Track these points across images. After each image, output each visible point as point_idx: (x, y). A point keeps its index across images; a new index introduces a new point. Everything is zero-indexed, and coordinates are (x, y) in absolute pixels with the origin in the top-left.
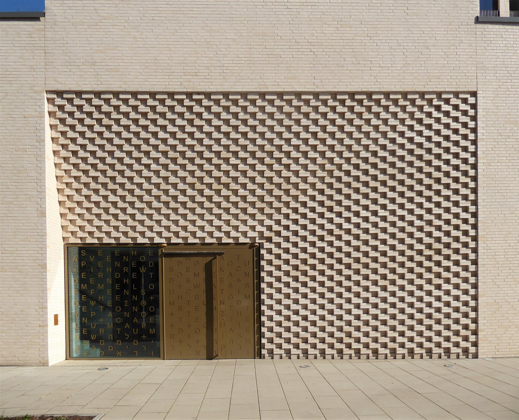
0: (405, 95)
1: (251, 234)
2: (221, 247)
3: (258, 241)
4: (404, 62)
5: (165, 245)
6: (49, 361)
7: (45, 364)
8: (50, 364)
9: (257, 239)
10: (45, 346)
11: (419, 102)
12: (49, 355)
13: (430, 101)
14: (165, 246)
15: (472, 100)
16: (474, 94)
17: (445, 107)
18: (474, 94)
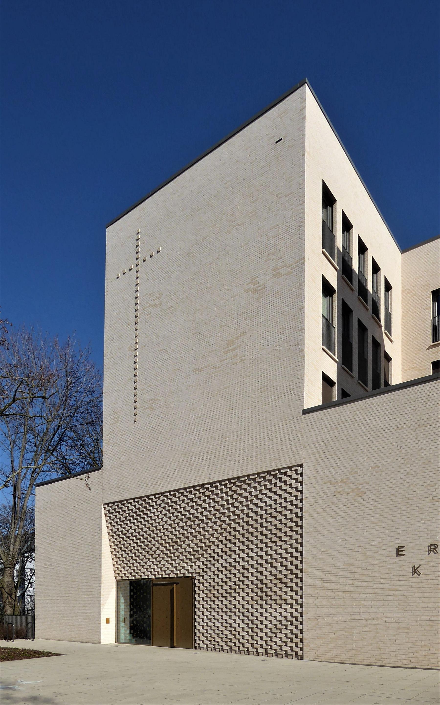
0: (258, 474)
1: (191, 571)
2: (178, 579)
3: (194, 575)
4: (257, 453)
5: (154, 579)
6: (102, 642)
7: (100, 643)
8: (102, 643)
9: (194, 573)
10: (100, 633)
11: (268, 478)
12: (102, 639)
13: (275, 476)
14: (153, 580)
15: (300, 470)
16: (301, 466)
17: (284, 478)
18: (301, 466)
